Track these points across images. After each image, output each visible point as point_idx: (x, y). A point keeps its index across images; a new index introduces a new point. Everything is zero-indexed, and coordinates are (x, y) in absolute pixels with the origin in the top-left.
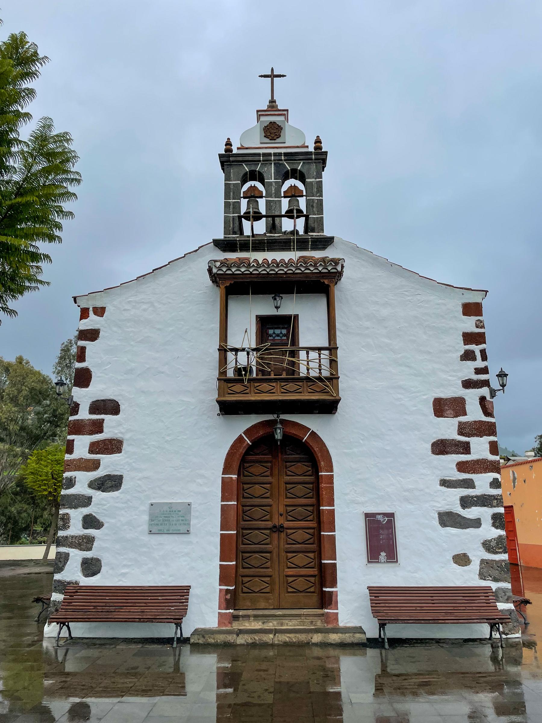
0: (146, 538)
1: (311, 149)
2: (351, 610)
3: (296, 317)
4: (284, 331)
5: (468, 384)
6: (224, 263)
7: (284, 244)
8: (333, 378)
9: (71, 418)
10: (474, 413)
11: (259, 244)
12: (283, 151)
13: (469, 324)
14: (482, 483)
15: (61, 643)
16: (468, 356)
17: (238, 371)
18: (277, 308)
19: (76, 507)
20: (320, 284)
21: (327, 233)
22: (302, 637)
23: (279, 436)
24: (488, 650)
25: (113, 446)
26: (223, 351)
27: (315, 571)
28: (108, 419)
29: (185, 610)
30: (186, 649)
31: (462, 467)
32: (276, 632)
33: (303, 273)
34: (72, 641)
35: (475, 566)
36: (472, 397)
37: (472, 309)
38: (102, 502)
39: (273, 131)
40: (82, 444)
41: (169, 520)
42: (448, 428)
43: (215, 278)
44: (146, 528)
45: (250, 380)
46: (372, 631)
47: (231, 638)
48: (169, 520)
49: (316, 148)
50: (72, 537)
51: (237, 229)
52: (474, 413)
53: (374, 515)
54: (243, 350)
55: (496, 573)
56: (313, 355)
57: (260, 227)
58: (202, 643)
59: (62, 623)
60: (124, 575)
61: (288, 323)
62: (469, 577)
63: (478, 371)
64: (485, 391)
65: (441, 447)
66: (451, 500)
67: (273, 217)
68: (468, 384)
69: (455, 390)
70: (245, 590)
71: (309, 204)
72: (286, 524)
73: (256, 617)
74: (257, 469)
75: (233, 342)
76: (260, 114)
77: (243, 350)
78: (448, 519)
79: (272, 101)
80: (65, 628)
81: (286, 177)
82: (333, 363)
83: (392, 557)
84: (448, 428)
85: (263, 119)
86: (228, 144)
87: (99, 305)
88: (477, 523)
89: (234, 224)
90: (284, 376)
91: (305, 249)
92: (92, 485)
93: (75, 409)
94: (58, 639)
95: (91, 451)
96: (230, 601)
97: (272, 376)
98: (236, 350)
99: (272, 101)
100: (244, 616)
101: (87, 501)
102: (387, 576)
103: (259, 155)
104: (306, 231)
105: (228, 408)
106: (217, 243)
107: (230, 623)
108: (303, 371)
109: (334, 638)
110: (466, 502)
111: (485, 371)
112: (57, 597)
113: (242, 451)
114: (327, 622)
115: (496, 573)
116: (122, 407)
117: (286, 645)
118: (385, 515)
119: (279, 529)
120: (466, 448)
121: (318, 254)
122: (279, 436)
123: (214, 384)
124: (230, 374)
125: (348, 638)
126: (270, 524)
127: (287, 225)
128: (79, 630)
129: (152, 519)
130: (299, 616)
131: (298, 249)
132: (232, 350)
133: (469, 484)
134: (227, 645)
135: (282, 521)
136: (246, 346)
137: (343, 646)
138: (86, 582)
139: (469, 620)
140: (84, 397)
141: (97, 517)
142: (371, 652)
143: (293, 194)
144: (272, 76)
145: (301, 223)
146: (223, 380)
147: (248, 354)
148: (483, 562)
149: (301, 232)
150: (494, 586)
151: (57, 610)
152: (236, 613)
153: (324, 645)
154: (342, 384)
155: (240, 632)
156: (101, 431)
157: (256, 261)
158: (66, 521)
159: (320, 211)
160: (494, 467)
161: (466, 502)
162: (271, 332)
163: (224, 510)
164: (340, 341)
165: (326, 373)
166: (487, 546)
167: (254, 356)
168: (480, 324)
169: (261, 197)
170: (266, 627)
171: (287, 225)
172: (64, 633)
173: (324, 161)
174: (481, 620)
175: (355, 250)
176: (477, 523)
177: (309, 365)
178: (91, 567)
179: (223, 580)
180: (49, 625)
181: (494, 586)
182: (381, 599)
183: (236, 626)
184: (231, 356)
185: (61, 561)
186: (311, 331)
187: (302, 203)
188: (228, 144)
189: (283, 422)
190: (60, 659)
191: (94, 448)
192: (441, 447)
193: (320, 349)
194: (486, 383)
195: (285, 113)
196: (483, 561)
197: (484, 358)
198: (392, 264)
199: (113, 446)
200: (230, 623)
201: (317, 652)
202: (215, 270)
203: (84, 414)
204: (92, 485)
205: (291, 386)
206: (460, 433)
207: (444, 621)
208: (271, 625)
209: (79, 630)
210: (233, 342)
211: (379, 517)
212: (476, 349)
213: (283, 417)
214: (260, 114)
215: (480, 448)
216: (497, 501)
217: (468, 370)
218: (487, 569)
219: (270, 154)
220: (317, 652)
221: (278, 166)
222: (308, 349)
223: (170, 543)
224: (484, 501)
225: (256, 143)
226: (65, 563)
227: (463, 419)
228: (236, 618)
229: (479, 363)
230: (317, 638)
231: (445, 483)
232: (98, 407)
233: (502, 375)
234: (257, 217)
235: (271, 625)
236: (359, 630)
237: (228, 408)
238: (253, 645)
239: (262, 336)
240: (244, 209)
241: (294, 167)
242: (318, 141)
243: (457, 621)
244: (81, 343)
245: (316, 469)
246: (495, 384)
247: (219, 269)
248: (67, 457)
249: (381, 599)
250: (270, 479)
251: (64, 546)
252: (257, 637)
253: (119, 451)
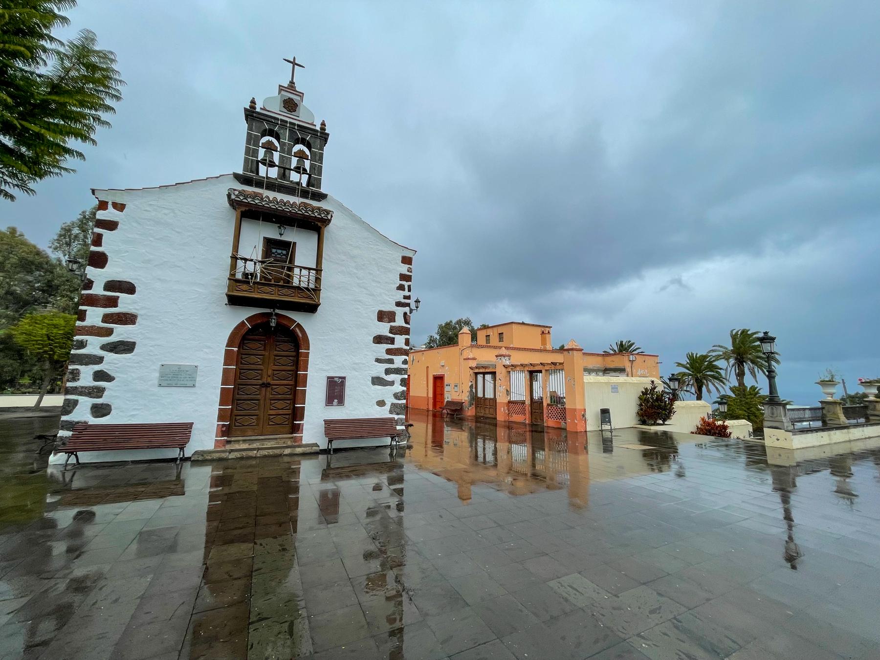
0: (157, 390)
1: (318, 128)
2: (312, 432)
3: (295, 244)
4: (284, 252)
5: (399, 304)
6: (241, 193)
7: (291, 190)
8: (317, 290)
9: (83, 292)
10: (400, 322)
11: (271, 185)
12: (297, 122)
13: (404, 269)
14: (398, 361)
15: (69, 468)
16: (401, 288)
17: (246, 275)
18: (281, 235)
19: (86, 364)
20: (315, 224)
21: (323, 190)
22: (277, 452)
23: (273, 324)
24: (388, 451)
25: (128, 319)
26: (234, 258)
27: (290, 412)
28: (123, 297)
29: (188, 439)
30: (189, 464)
31: (389, 352)
32: (259, 449)
33: (303, 214)
34: (79, 466)
35: (388, 407)
36: (400, 311)
37: (407, 260)
38: (112, 362)
39: (290, 105)
40: (94, 316)
41: (176, 377)
42: (384, 329)
43: (233, 203)
44: (156, 382)
45: (255, 283)
46: (323, 444)
47: (224, 455)
48: (176, 377)
49: (321, 129)
50: (82, 387)
51: (254, 169)
53: (333, 378)
54: (252, 260)
55: (398, 410)
56: (305, 272)
57: (273, 173)
58: (200, 460)
59: (70, 453)
60: (133, 416)
61: (288, 247)
62: (383, 413)
63: (405, 297)
64: (407, 309)
65: (379, 340)
66: (379, 370)
67: (285, 169)
68: (399, 304)
69: (390, 307)
70: (237, 424)
71: (312, 166)
72: (272, 382)
73: (244, 441)
74: (252, 345)
75: (242, 253)
76: (281, 88)
77: (252, 260)
78: (377, 381)
79: (292, 82)
80: (73, 457)
81: (297, 141)
82: (318, 280)
83: (341, 402)
84: (384, 329)
85: (283, 92)
86: (253, 102)
87: (119, 201)
88: (392, 383)
89: (252, 164)
90: (281, 283)
91: (307, 198)
92: (104, 347)
93: (89, 284)
94: (66, 465)
95: (104, 321)
96: (226, 431)
97: (273, 282)
98: (246, 260)
99: (292, 82)
100: (234, 441)
101: (99, 360)
102: (337, 413)
103: (278, 119)
104: (309, 184)
105: (234, 301)
106: (237, 176)
107: (224, 446)
108: (296, 282)
109: (299, 450)
110: (388, 372)
111: (408, 297)
112: (62, 433)
113: (244, 331)
114: (295, 442)
115: (398, 410)
116: (137, 289)
117: (265, 456)
118: (340, 378)
119: (266, 385)
120: (392, 341)
121: (315, 204)
122: (273, 324)
123: (226, 282)
124: (239, 276)
125: (308, 450)
126: (260, 382)
127: (294, 177)
128: (85, 457)
129: (163, 376)
130: (276, 439)
131: (301, 197)
132: (242, 259)
133: (391, 361)
134: (220, 460)
135: (269, 380)
136: (254, 258)
137: (304, 455)
139: (381, 436)
140: (98, 277)
141: (109, 373)
142: (321, 457)
143: (301, 156)
144: (294, 63)
145: (305, 179)
146: (232, 279)
147: (255, 264)
148: (393, 405)
149: (304, 185)
150: (396, 417)
151: (64, 444)
152: (229, 439)
153: (291, 455)
154: (323, 294)
155: (232, 451)
156: (116, 306)
157: (268, 197)
158: (75, 375)
159: (320, 174)
160: (406, 353)
161: (388, 372)
162: (274, 251)
163: (225, 371)
164: (325, 265)
165: (312, 286)
166: (396, 396)
167: (259, 267)
168: (409, 270)
169: (276, 151)
170: (251, 447)
171: (294, 177)
172: (73, 460)
173: (326, 140)
174: (387, 435)
175: (341, 206)
176: (392, 383)
177: (301, 278)
178: (100, 410)
179: (221, 418)
180: (55, 454)
181: (396, 417)
182: (332, 428)
183: (228, 447)
184: (240, 263)
185: (70, 406)
186: (305, 255)
187: (307, 164)
188: (253, 102)
189: (277, 315)
190: (67, 479)
191: (107, 318)
192: (379, 340)
193: (310, 269)
194: (408, 305)
195: (301, 95)
196: (393, 405)
197: (409, 290)
198: (364, 222)
199: (128, 319)
200: (224, 446)
201: (286, 459)
202: (233, 197)
203: (98, 290)
204: (104, 347)
205: (285, 291)
206: (390, 332)
207: (367, 437)
208: (255, 445)
209: (85, 457)
210: (242, 253)
211: (336, 379)
212: (406, 284)
213: (277, 311)
214: (281, 88)
215: (400, 341)
216: (405, 371)
217: (400, 296)
218: (394, 408)
219: (286, 122)
220: (286, 459)
221: (292, 132)
222: (301, 268)
223: (177, 394)
224: (398, 371)
225: (276, 109)
226: (74, 408)
227: (393, 324)
228: (229, 442)
229: (406, 293)
230: (287, 451)
231: (378, 360)
232: (111, 286)
233: (417, 301)
234: (272, 164)
235: (255, 445)
236: (316, 445)
237: (234, 301)
238: (242, 458)
239: (267, 253)
240: (261, 156)
241: (304, 137)
242: (323, 124)
243: (375, 436)
244: (97, 230)
245: (297, 347)
246: (413, 306)
247: (237, 196)
248: (78, 323)
249: (332, 428)
250: (263, 353)
251: (72, 394)
252: (244, 454)
253: (133, 323)
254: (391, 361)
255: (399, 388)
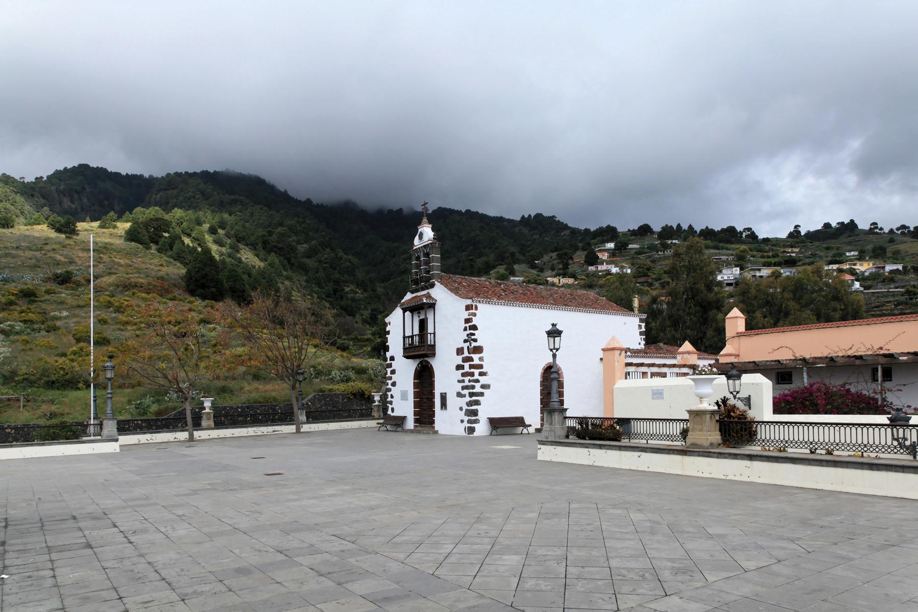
5: (465, 341)
10: (466, 354)
42: (459, 360)
52: (466, 354)
64: (468, 344)
68: (465, 341)
69: (461, 344)
83: (446, 408)
88: (464, 396)
110: (463, 388)
133: (463, 381)
138: (392, 414)
140: (388, 355)
161: (463, 388)
176: (464, 396)
184: (407, 340)
192: (459, 367)
203: (389, 362)
212: (467, 325)
229: (468, 332)
231: (459, 381)
254: (463, 381)
255: (468, 399)
